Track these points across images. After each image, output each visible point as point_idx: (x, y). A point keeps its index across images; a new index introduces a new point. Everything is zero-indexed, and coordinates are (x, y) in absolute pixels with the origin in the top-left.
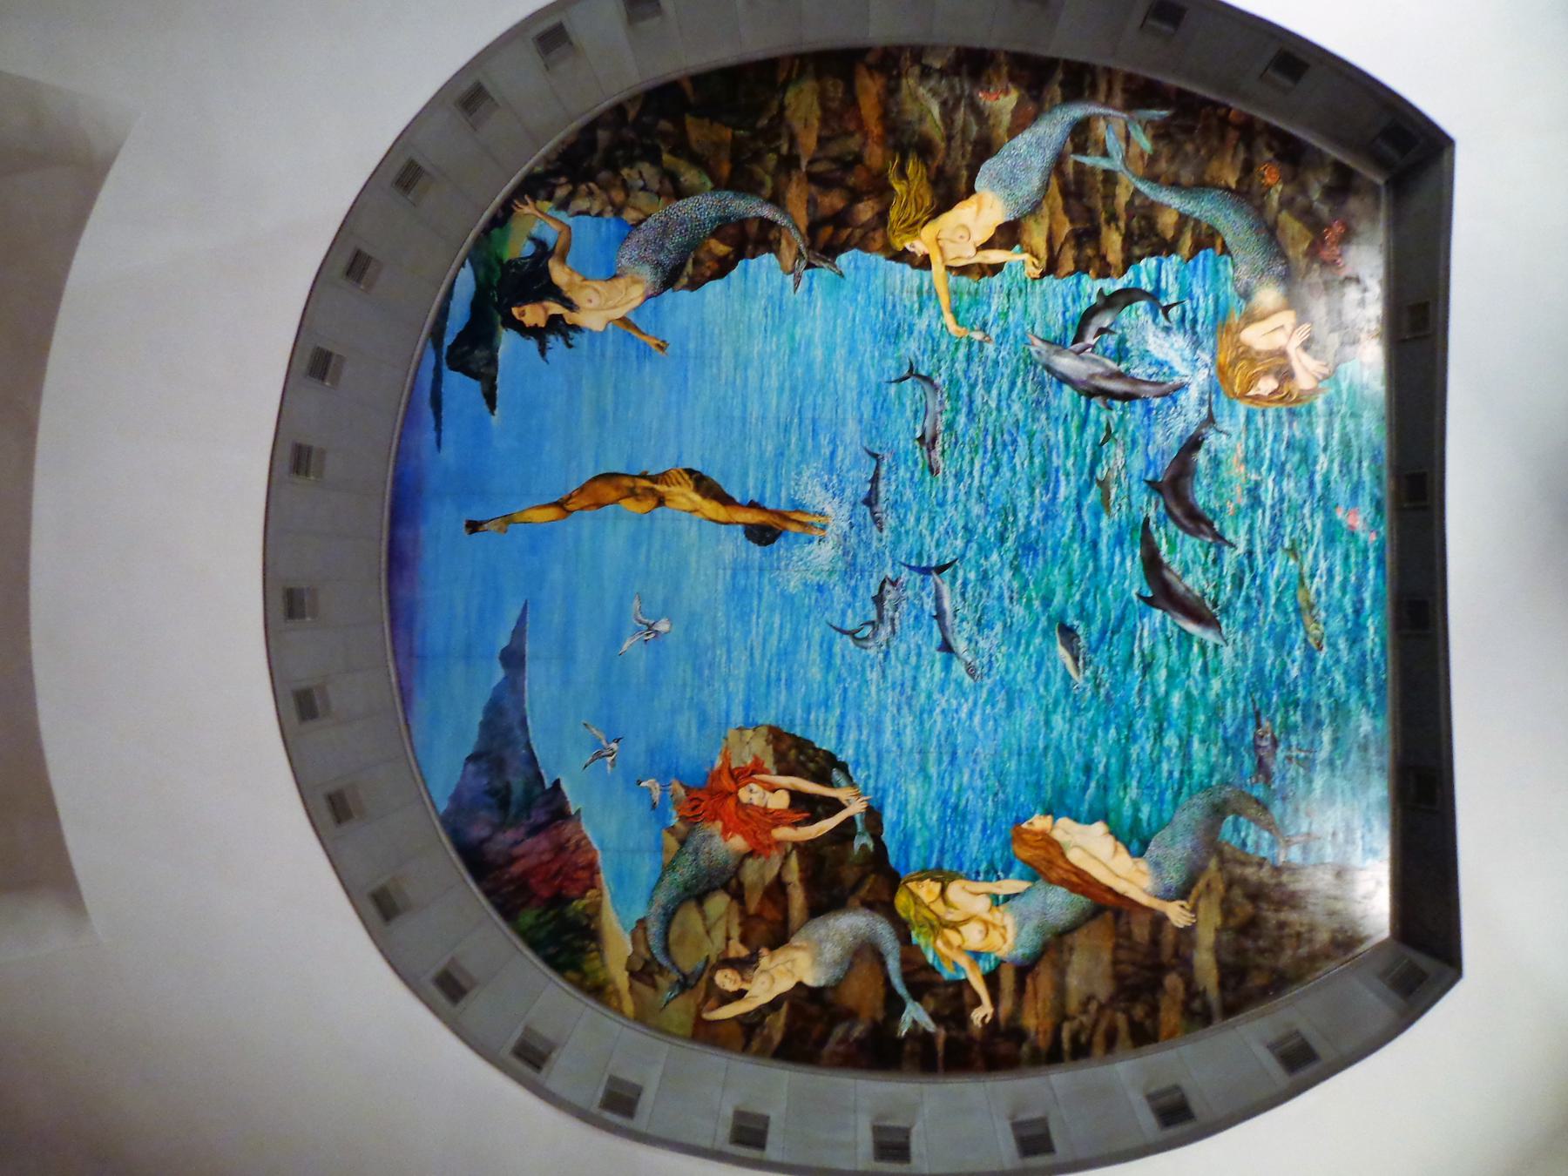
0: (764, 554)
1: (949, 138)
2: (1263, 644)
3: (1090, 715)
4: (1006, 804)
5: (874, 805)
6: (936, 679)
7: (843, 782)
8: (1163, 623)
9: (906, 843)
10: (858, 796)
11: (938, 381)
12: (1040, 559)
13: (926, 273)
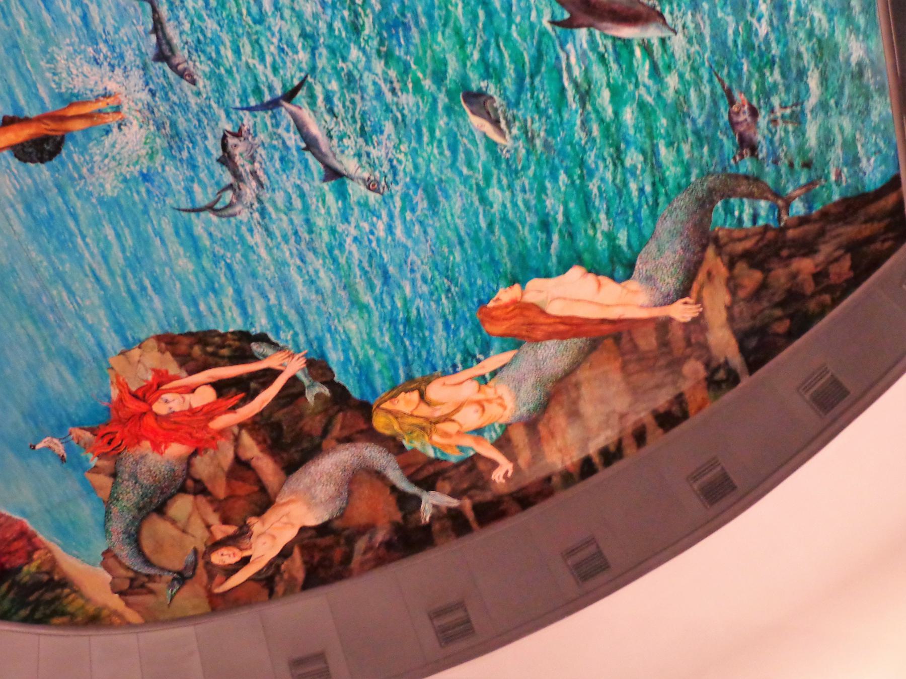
0: (54, 170)
2: (720, 14)
3: (530, 173)
4: (463, 295)
5: (314, 356)
6: (334, 211)
7: (268, 351)
8: (592, 41)
9: (364, 373)
10: (292, 356)
12: (414, 32)
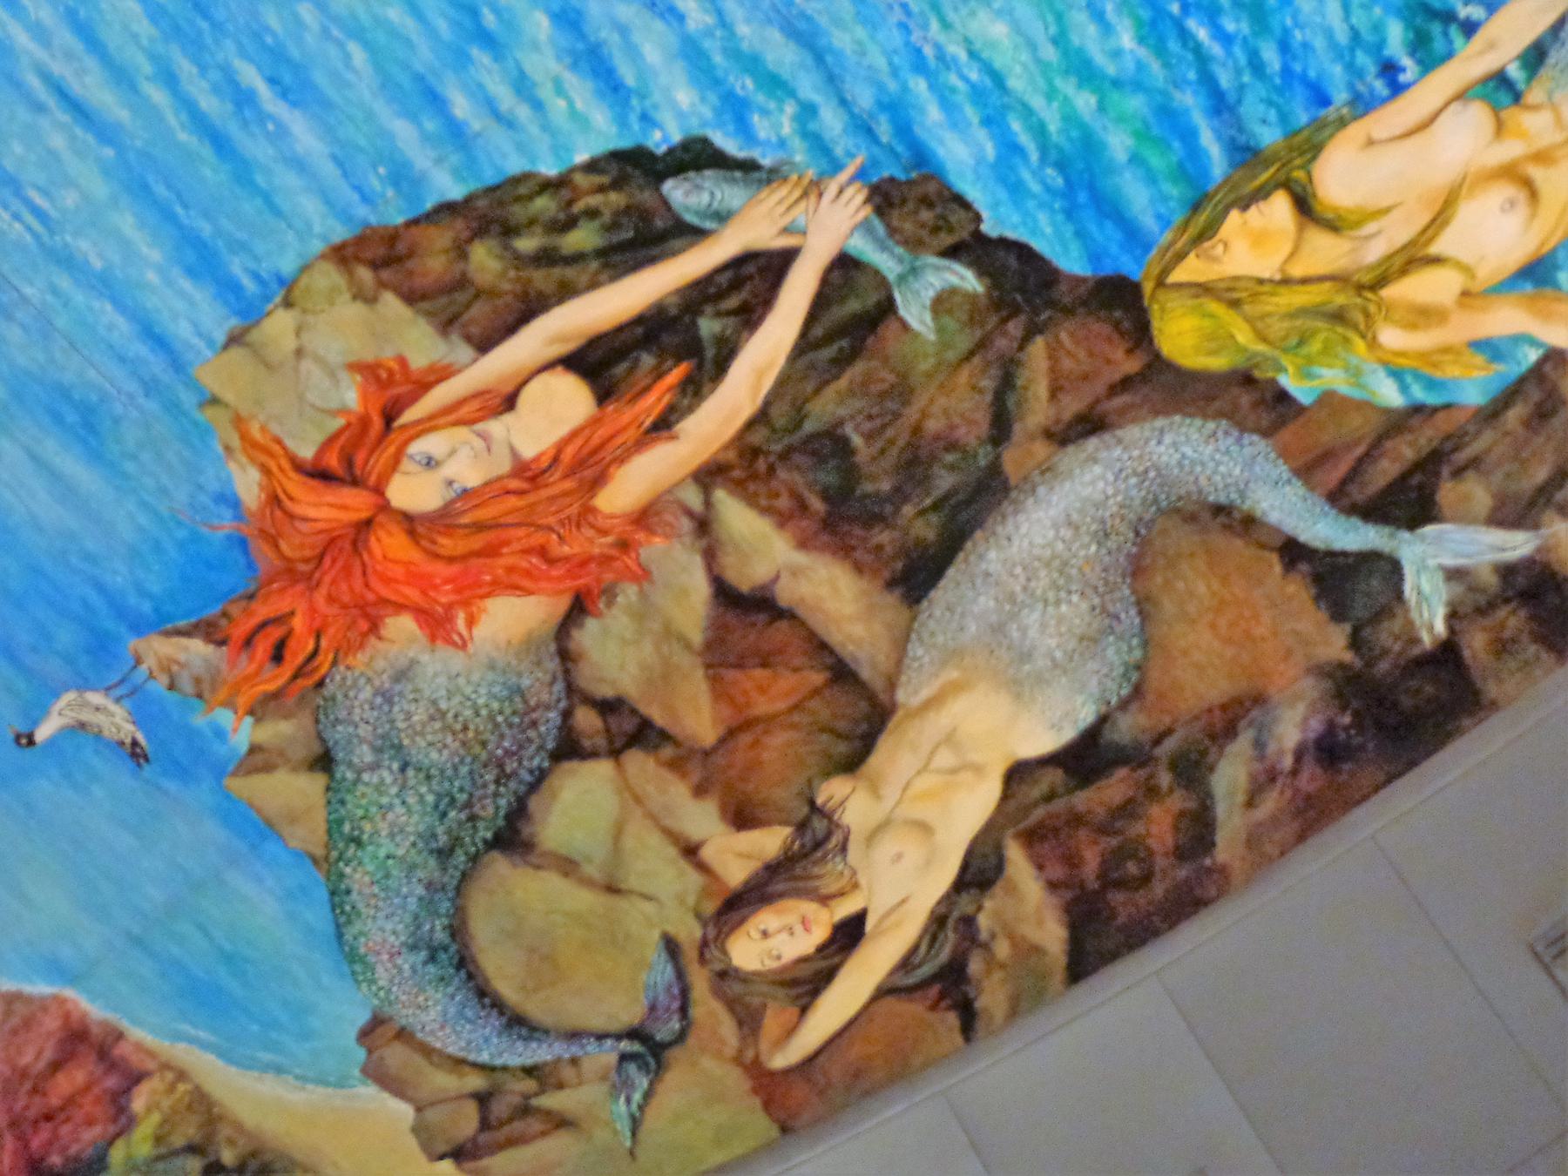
10: (814, 188)
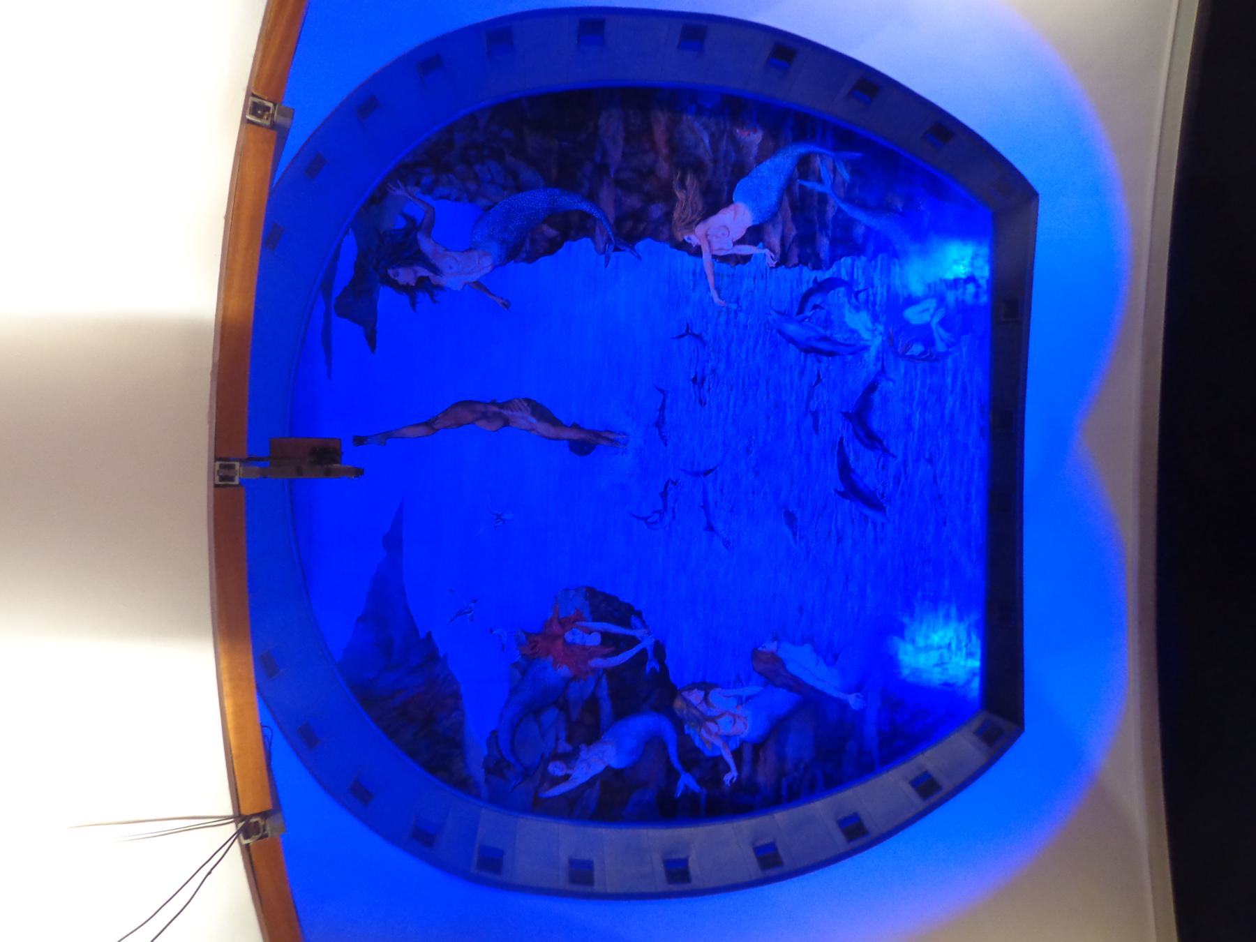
1: (715, 161)
10: (649, 634)
11: (706, 338)
13: (698, 260)
